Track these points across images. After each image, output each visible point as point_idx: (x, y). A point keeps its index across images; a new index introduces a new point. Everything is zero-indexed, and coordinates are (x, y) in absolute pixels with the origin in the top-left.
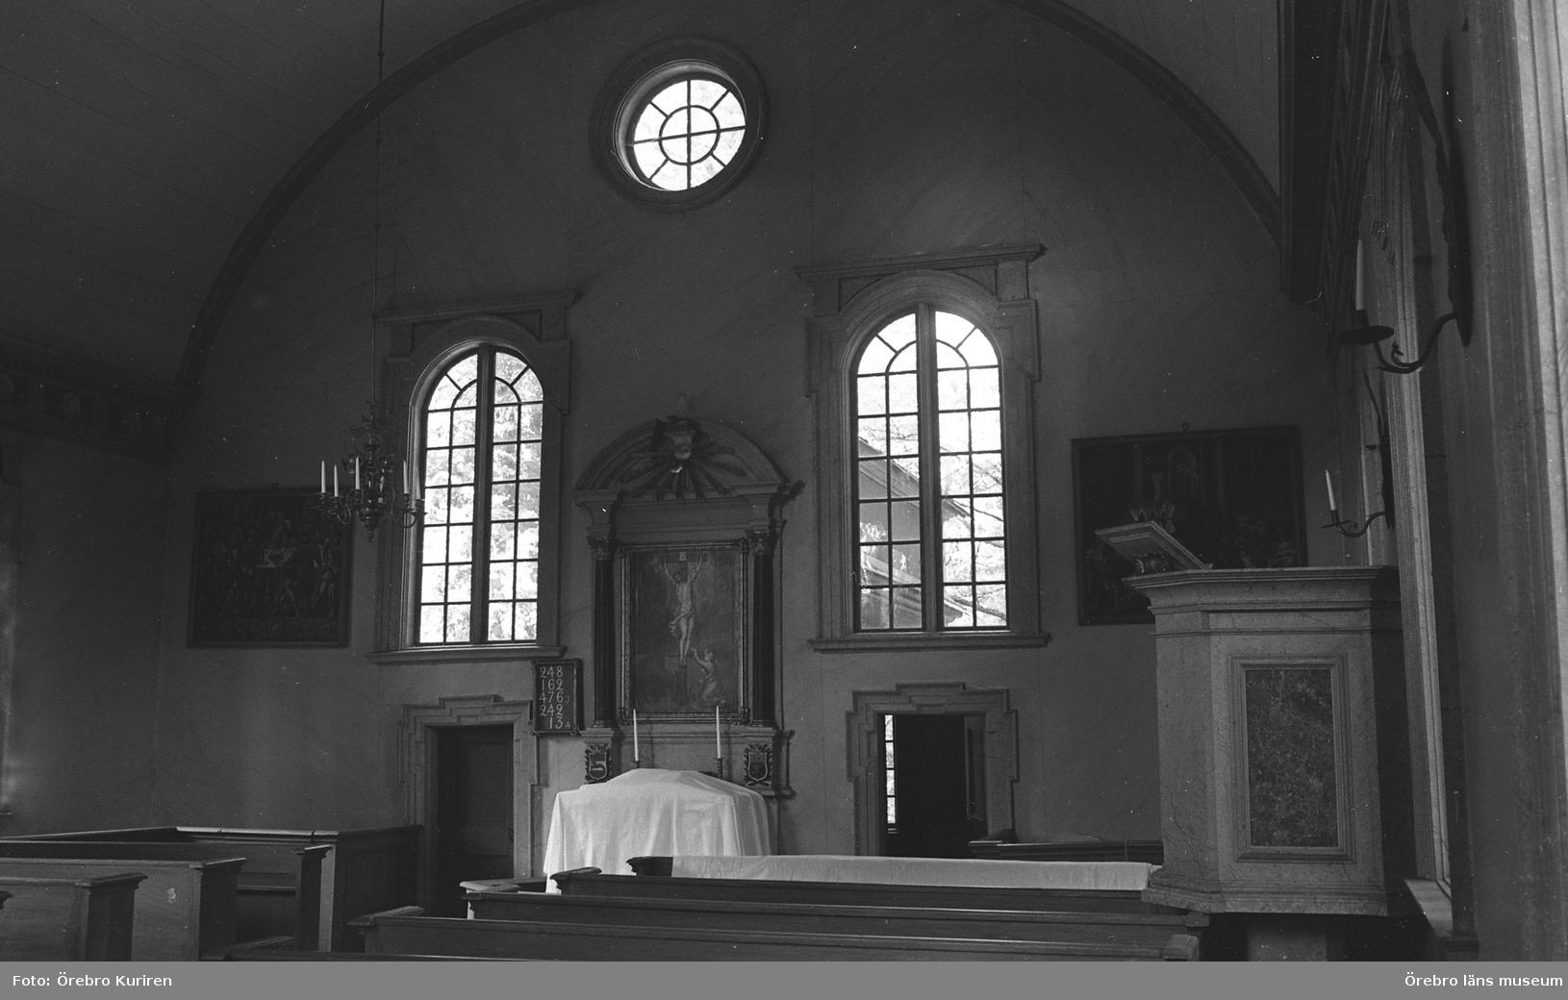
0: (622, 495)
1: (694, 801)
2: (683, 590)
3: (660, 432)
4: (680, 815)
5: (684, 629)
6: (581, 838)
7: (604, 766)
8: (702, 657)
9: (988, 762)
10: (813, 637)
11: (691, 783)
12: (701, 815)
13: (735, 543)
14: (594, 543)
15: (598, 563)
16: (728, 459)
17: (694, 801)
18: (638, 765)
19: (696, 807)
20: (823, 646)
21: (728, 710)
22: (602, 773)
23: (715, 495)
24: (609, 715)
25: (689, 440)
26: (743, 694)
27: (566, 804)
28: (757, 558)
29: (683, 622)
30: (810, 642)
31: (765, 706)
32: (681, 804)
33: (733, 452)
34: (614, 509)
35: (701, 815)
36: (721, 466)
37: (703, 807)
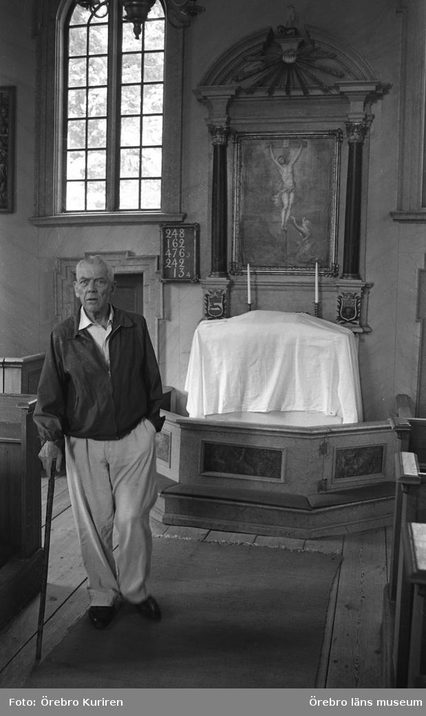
0: (239, 91)
1: (314, 339)
2: (286, 172)
3: (271, 39)
4: (302, 346)
5: (286, 202)
6: (216, 366)
7: (220, 308)
8: (300, 223)
9: (419, 335)
10: (394, 209)
11: (307, 323)
12: (320, 349)
13: (332, 133)
14: (213, 131)
15: (215, 147)
16: (330, 63)
17: (314, 339)
18: (251, 308)
19: (316, 343)
20: (402, 217)
21: (324, 264)
22: (217, 312)
23: (319, 92)
24: (221, 267)
25: (295, 46)
26: (336, 256)
27: (204, 338)
28: (350, 144)
29: (285, 196)
30: (392, 214)
31: (353, 266)
32: (303, 340)
33: (333, 57)
34: (231, 102)
35: (320, 349)
36: (323, 70)
37: (322, 343)
